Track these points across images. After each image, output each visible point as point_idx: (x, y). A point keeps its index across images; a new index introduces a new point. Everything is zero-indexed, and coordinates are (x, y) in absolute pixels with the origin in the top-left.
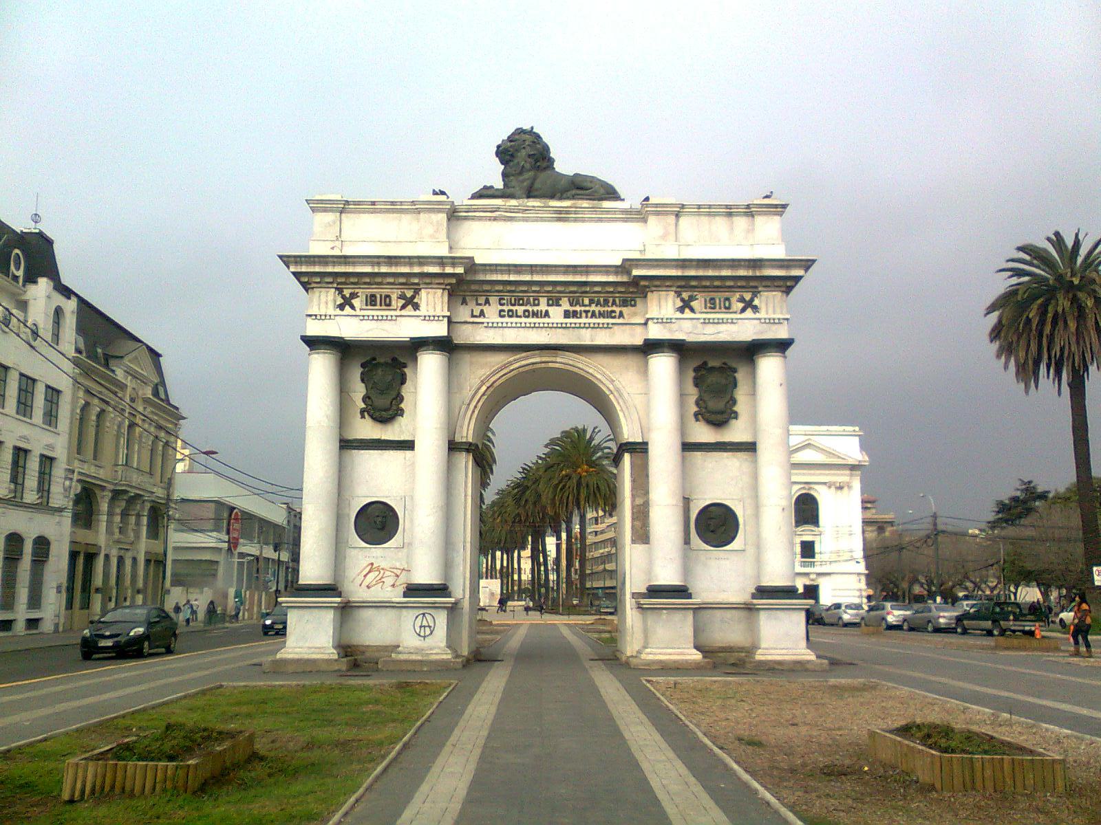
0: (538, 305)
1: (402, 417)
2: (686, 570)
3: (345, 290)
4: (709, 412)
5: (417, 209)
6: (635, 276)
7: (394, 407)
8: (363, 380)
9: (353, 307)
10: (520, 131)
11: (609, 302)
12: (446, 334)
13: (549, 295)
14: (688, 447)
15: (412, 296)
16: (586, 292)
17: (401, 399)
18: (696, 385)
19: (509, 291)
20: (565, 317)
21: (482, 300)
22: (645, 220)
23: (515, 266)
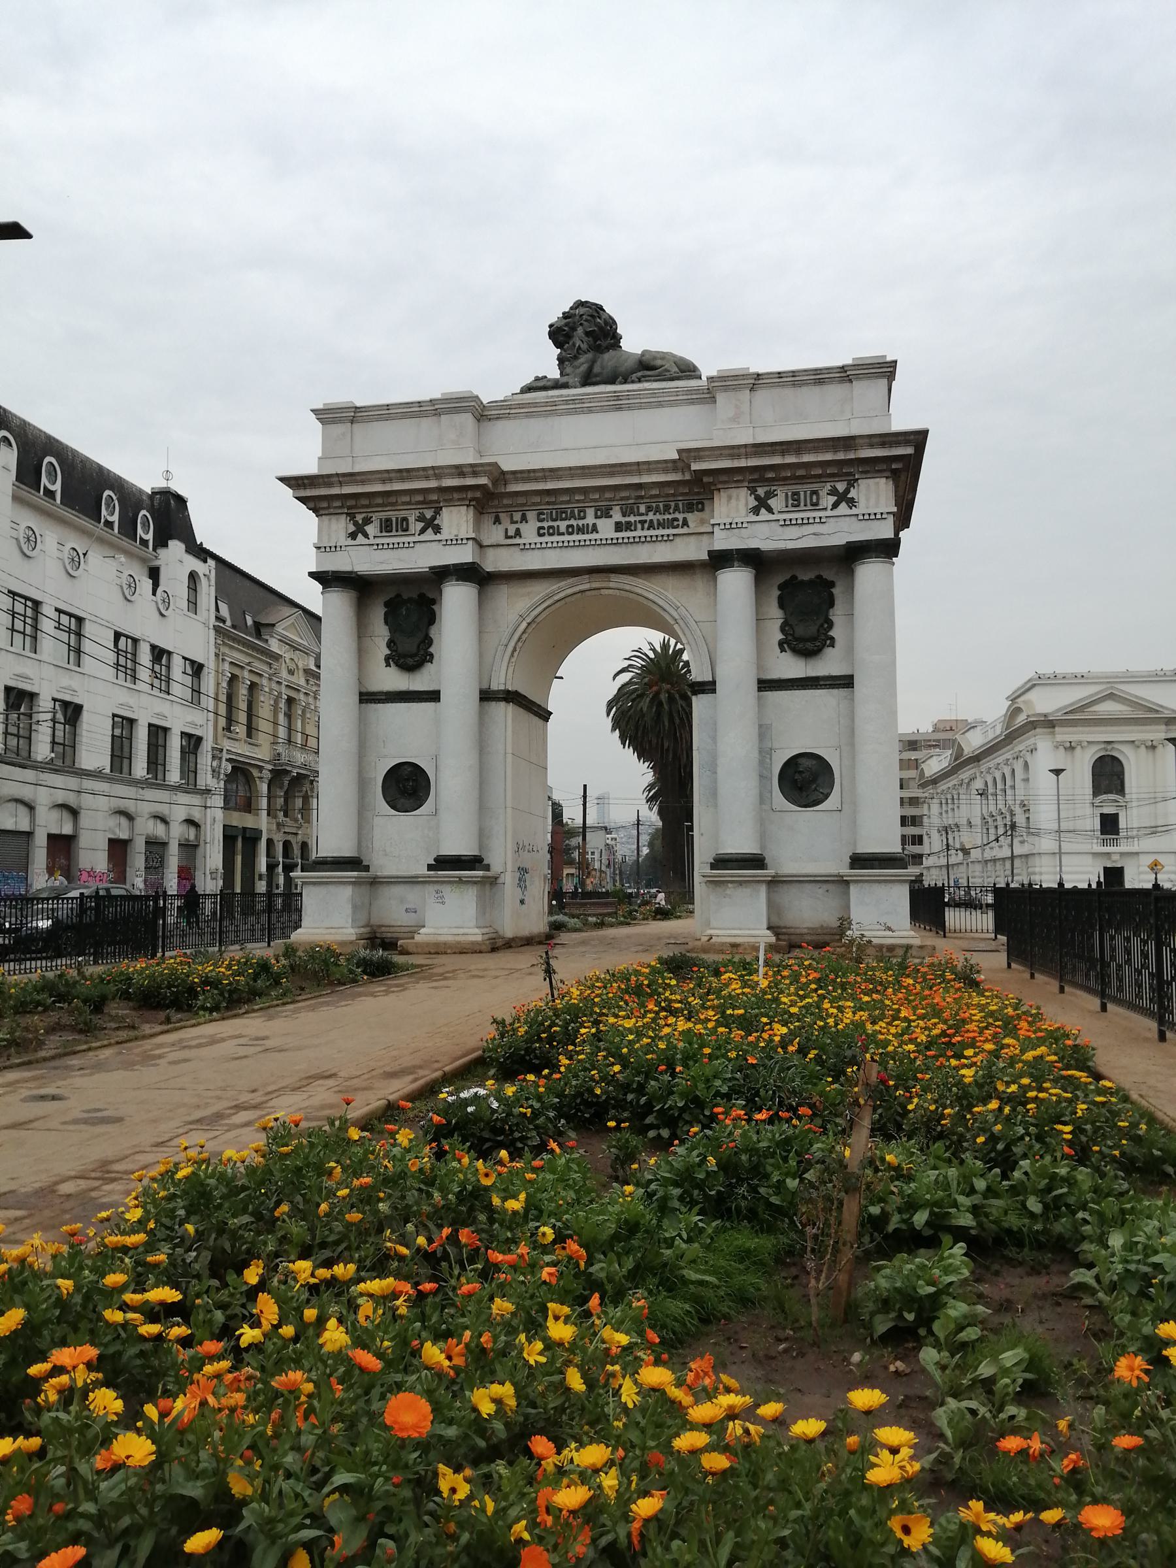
0: (584, 518)
2: (763, 836)
4: (796, 639)
7: (422, 652)
8: (386, 623)
9: (366, 536)
10: (580, 304)
14: (766, 685)
16: (642, 497)
17: (430, 642)
18: (782, 605)
19: (548, 503)
21: (517, 516)
22: (713, 400)
23: (551, 470)
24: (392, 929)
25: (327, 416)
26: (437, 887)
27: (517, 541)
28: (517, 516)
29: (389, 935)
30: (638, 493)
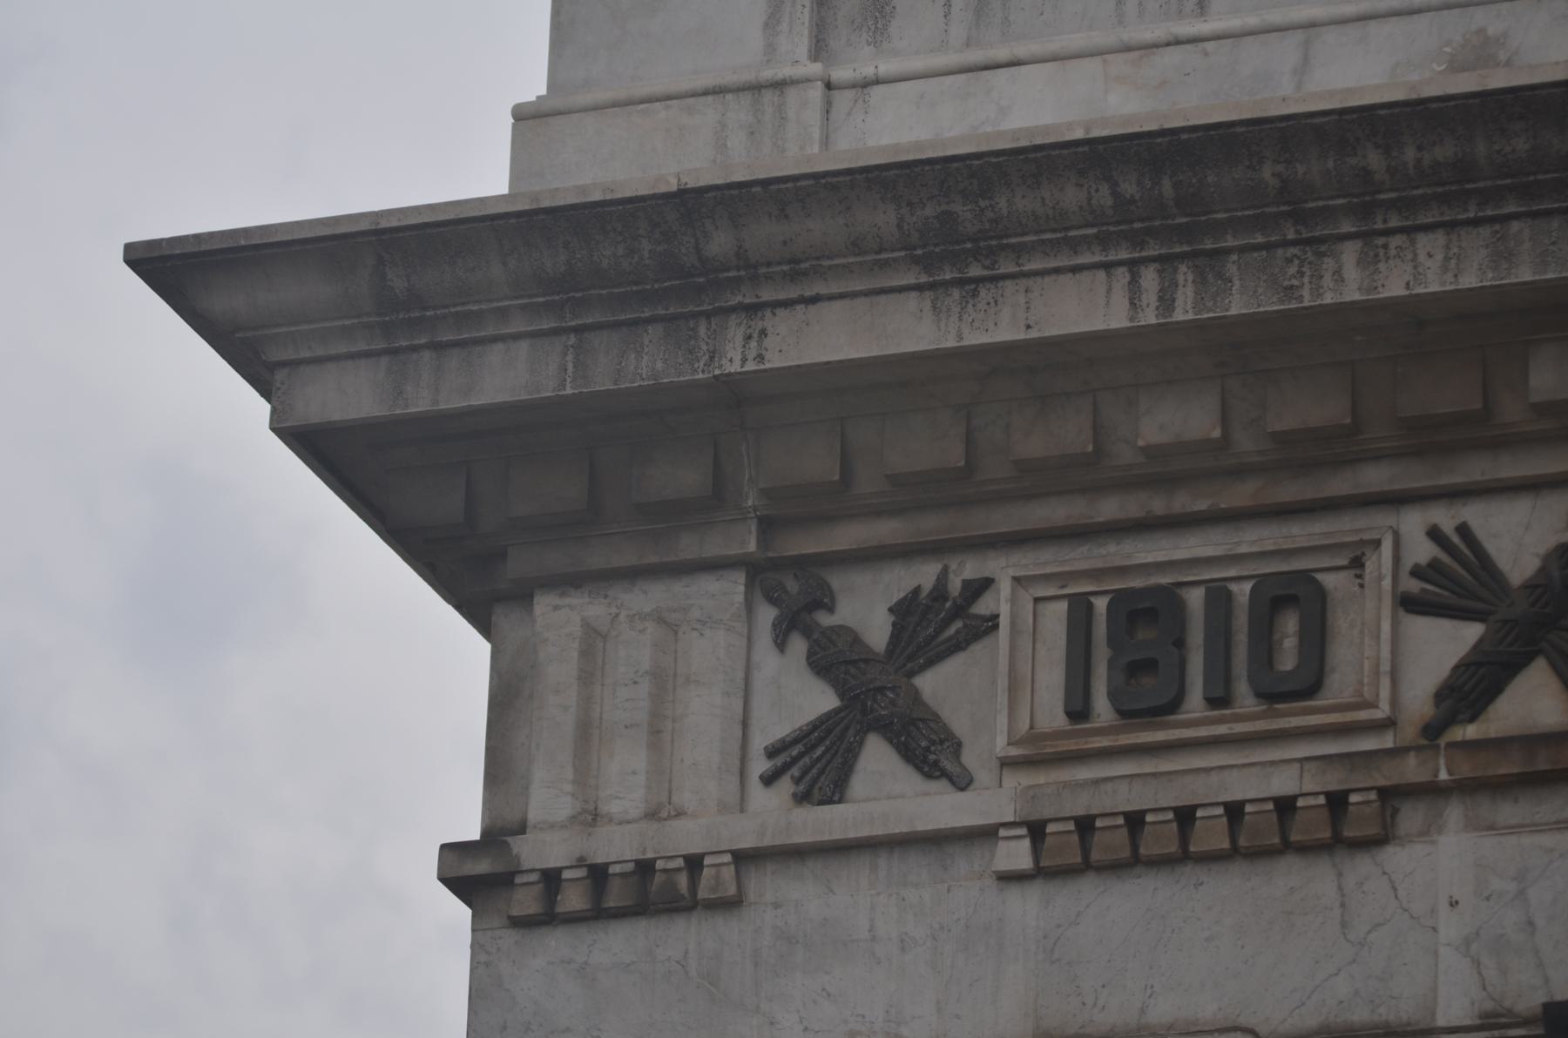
3: (836, 580)
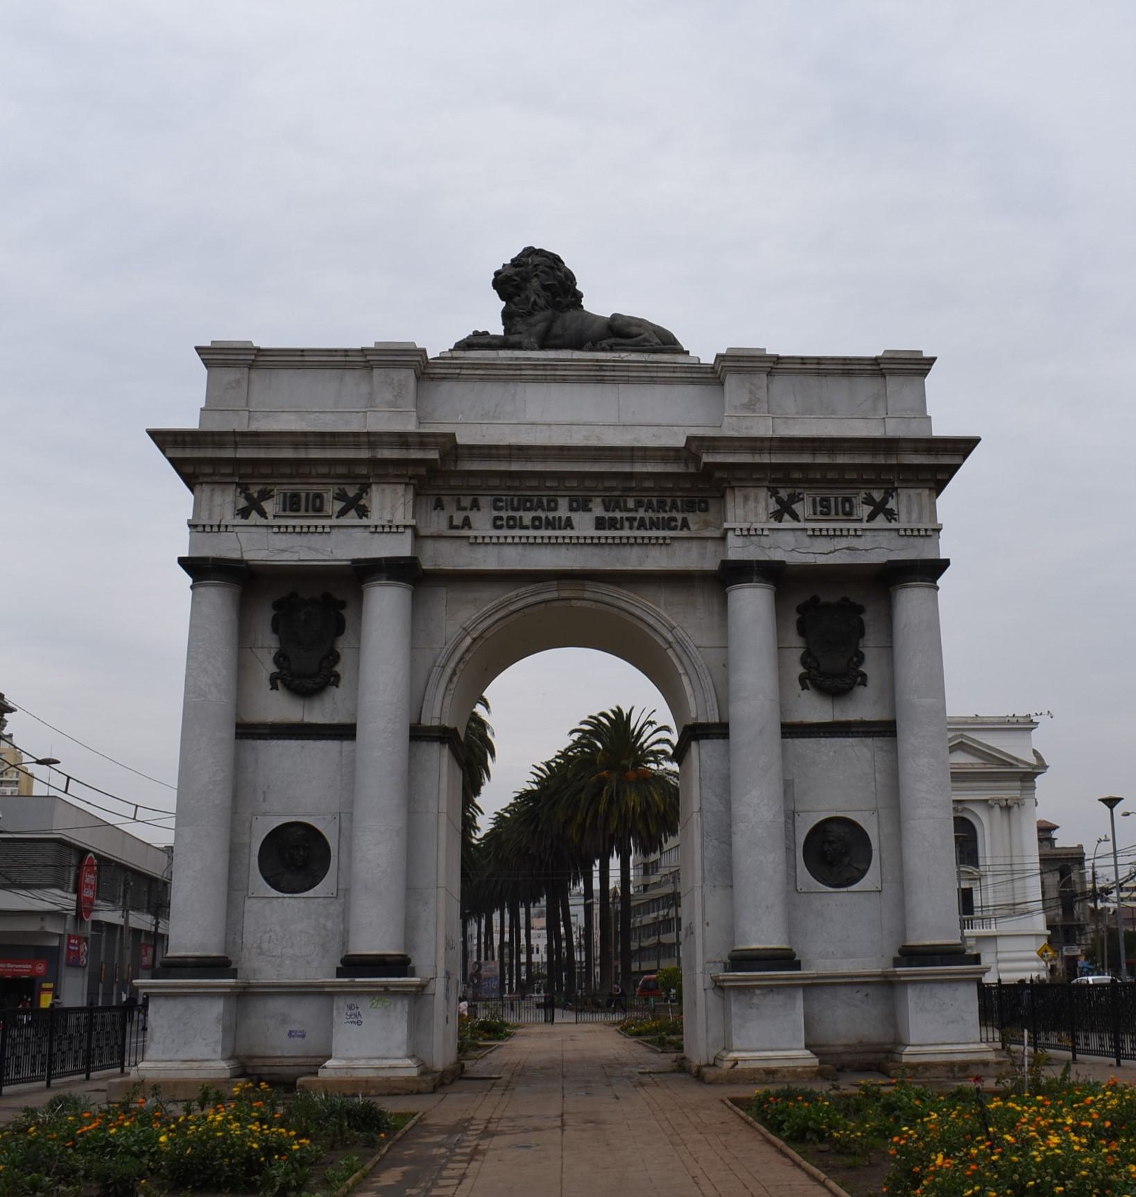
0: (555, 509)
1: (337, 686)
5: (368, 361)
6: (705, 463)
8: (275, 630)
9: (263, 514)
11: (666, 505)
12: (409, 554)
13: (572, 493)
14: (791, 730)
15: (357, 494)
16: (631, 489)
17: (335, 657)
18: (802, 631)
19: (509, 488)
20: (597, 528)
21: (466, 502)
23: (521, 448)
24: (269, 1062)
25: (215, 356)
26: (350, 1001)
27: (466, 532)
28: (466, 502)
29: (265, 1070)
30: (628, 485)
